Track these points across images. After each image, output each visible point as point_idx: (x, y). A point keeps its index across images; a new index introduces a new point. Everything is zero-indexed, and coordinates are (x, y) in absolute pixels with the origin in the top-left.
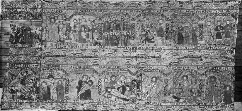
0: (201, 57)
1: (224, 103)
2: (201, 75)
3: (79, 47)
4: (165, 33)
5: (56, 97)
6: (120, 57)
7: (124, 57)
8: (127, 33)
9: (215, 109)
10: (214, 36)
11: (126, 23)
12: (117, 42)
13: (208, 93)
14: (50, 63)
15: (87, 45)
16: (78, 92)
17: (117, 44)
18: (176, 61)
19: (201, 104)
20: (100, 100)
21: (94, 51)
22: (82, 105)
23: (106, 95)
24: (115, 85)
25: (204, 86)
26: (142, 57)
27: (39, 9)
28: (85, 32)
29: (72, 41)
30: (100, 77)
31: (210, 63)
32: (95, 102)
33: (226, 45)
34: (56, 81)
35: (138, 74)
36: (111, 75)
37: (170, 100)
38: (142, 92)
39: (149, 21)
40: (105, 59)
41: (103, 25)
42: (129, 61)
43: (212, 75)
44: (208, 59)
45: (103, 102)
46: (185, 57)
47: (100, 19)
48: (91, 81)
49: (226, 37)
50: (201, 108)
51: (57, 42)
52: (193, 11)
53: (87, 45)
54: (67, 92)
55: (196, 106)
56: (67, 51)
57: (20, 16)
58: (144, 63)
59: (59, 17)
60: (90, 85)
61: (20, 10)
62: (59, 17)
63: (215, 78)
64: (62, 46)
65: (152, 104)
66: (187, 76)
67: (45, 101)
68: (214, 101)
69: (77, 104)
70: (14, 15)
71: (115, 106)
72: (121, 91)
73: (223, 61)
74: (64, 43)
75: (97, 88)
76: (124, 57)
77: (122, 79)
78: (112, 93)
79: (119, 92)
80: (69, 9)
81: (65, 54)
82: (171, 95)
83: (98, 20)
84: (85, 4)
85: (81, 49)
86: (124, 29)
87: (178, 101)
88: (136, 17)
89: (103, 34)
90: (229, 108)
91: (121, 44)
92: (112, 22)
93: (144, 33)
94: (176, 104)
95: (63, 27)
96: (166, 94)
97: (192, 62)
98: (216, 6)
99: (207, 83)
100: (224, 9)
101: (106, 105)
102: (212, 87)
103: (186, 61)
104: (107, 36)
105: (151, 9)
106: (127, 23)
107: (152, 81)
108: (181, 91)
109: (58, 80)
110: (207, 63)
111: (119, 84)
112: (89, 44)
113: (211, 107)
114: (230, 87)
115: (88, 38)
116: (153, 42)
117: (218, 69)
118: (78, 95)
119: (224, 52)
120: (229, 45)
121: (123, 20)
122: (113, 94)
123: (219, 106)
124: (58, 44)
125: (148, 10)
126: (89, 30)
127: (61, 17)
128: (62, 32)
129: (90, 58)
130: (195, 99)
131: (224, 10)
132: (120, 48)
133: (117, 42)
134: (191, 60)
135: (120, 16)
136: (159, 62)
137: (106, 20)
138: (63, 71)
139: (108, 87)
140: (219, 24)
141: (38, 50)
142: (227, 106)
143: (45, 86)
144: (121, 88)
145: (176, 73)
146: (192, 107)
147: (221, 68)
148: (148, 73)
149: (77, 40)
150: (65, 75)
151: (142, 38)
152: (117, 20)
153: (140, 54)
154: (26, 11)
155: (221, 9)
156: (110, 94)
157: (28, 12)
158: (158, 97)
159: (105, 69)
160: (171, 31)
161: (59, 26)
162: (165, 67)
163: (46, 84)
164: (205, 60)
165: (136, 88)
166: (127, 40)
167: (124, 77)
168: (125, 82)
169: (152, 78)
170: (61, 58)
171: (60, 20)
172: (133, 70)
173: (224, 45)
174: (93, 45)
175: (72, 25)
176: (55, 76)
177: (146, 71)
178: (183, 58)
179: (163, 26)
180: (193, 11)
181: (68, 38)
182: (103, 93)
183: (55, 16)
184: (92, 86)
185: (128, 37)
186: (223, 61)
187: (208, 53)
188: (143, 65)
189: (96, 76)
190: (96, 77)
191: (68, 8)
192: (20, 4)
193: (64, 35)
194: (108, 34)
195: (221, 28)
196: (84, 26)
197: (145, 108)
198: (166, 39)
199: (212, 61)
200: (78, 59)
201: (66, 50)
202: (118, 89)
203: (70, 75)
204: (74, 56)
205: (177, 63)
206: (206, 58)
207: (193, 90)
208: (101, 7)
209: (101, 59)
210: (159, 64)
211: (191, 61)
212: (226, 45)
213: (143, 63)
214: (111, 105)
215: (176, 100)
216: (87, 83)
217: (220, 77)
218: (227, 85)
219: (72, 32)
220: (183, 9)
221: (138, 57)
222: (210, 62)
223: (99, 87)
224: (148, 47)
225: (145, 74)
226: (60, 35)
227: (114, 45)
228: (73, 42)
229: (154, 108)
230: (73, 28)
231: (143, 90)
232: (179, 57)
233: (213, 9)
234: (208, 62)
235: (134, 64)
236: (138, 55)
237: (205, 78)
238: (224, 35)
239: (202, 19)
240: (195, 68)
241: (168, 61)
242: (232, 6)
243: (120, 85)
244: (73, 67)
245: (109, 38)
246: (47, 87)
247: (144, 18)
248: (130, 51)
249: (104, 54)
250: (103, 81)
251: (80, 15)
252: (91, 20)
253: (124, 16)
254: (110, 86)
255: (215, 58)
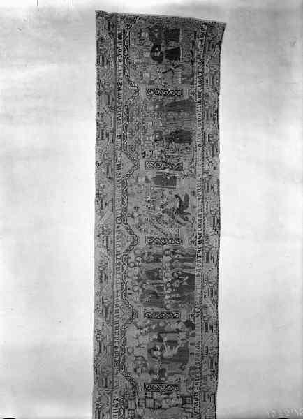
3: (196, 363)
4: (167, 171)
8: (167, 255)
10: (173, 65)
11: (145, 258)
12: (187, 278)
15: (191, 344)
17: (192, 278)
21: (207, 329)
28: (163, 348)
29: (183, 378)
33: (195, 38)
39: (140, 206)
41: (149, 309)
47: (134, 314)
49: (177, 39)
51: (186, 413)
52: (118, 110)
53: (191, 344)
56: (205, 390)
59: (130, 407)
62: (130, 407)
64: (194, 401)
74: (186, 397)
80: (111, 382)
83: (137, 320)
84: (100, 346)
85: (203, 358)
86: (158, 261)
88: (132, 233)
89: (168, 309)
91: (190, 268)
92: (141, 287)
93: (166, 217)
95: (152, 398)
98: (108, 62)
100: (115, 43)
104: (173, 299)
105: (113, 201)
106: (144, 254)
112: (191, 340)
115: (176, 342)
116: (187, 196)
119: (210, 43)
120: (195, 32)
121: (139, 262)
124: (190, 410)
125: (116, 208)
126: (160, 340)
127: (130, 402)
128: (164, 401)
131: (118, 45)
132: (199, 270)
133: (187, 278)
135: (129, 269)
137: (138, 300)
140: (148, 54)
149: (181, 368)
151: (178, 222)
152: (138, 276)
153: (214, 226)
155: (115, 52)
160: (162, 158)
161: (150, 408)
166: (182, 255)
171: (137, 404)
173: (193, 43)
174: (193, 332)
175: (148, 378)
179: (151, 174)
180: (118, 110)
181: (177, 387)
183: (127, 416)
185: (176, 253)
187: (210, 78)
191: (108, 385)
193: (171, 396)
194: (167, 297)
195: (157, 49)
196: (150, 351)
198: (179, 168)
208: (108, 312)
212: (195, 38)
219: (163, 379)
220: (113, 131)
224: (198, 208)
226: (170, 406)
227: (194, 284)
228: (186, 376)
230: (156, 377)
233: (115, 68)
238: (173, 44)
239: (136, 92)
242: (109, 28)
245: (178, 296)
247: (133, 216)
248: (207, 249)
251: (125, 359)
252: (137, 335)
253: (129, 261)
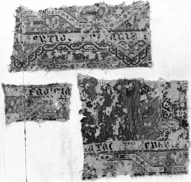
27: (142, 30)
57: (77, 57)
61: (75, 38)
70: (57, 54)
154: (96, 38)
157: (103, 44)
192: (76, 14)
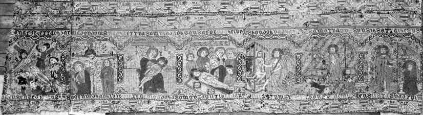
0: (360, 10)
1: (404, 93)
2: (362, 44)
5: (101, 89)
6: (214, 14)
7: (223, 14)
9: (388, 104)
13: (374, 77)
14: (89, 28)
16: (141, 78)
18: (316, 20)
19: (362, 97)
20: (179, 93)
22: (149, 102)
23: (191, 83)
24: (207, 65)
25: (366, 63)
26: (255, 14)
30: (180, 52)
31: (377, 21)
32: (171, 96)
34: (101, 60)
35: (249, 43)
36: (200, 47)
37: (307, 91)
38: (256, 76)
40: (188, 18)
42: (230, 20)
43: (381, 42)
44: (373, 14)
45: (185, 97)
46: (333, 12)
48: (163, 58)
50: (362, 104)
54: (120, 80)
55: (354, 99)
56: (119, 5)
58: (259, 23)
60: (162, 67)
63: (386, 48)
65: (273, 98)
66: (336, 46)
67: (81, 97)
68: (385, 90)
69: (140, 102)
71: (207, 103)
72: (218, 76)
73: (401, 17)
75: (175, 70)
76: (223, 14)
77: (218, 54)
78: (201, 79)
79: (215, 77)
81: (115, 10)
82: (309, 81)
87: (320, 92)
90: (412, 102)
94: (317, 98)
96: (299, 79)
97: (345, 21)
99: (373, 59)
101: (192, 102)
102: (381, 65)
103: (333, 20)
107: (273, 56)
108: (325, 72)
109: (104, 58)
110: (371, 21)
111: (214, 63)
113: (381, 102)
114: (415, 64)
117: (391, 32)
118: (140, 85)
122: (203, 81)
123: (394, 99)
129: (161, 16)
130: (351, 87)
134: (343, 17)
136: (285, 22)
138: (113, 42)
139: (193, 70)
141: (67, 4)
142: (410, 98)
143: (80, 69)
144: (218, 71)
145: (315, 41)
146: (347, 102)
147: (397, 31)
148: (265, 43)
150: (116, 49)
156: (197, 81)
158: (285, 84)
159: (188, 36)
162: (297, 31)
163: (83, 66)
164: (367, 16)
165: (244, 69)
167: (222, 51)
168: (224, 60)
169: (273, 52)
170: (108, 18)
172: (239, 38)
176: (98, 52)
177: (262, 39)
178: (329, 14)
182: (185, 81)
184: (164, 68)
186: (401, 17)
187: (373, 3)
188: (256, 27)
189: (172, 50)
190: (172, 52)
197: (262, 105)
199: (381, 18)
200: (138, 20)
201: (115, 3)
202: (213, 72)
203: (125, 49)
204: (132, 14)
205: (316, 22)
206: (369, 12)
207: (348, 72)
209: (180, 18)
210: (285, 25)
211: (342, 18)
213: (257, 23)
214: (200, 102)
215: (318, 89)
216: (156, 62)
217: (395, 47)
218: (409, 61)
221: (246, 13)
222: (377, 20)
223: (179, 70)
225: (260, 43)
229: (277, 105)
231: (258, 74)
232: (320, 12)
234: (374, 19)
235: (241, 26)
236: (248, 9)
237: (368, 49)
240: (350, 30)
241: (301, 19)
243: (216, 64)
244: (130, 34)
246: (84, 71)
249: (187, 9)
250: (185, 57)
254: (197, 67)
255: (386, 12)
